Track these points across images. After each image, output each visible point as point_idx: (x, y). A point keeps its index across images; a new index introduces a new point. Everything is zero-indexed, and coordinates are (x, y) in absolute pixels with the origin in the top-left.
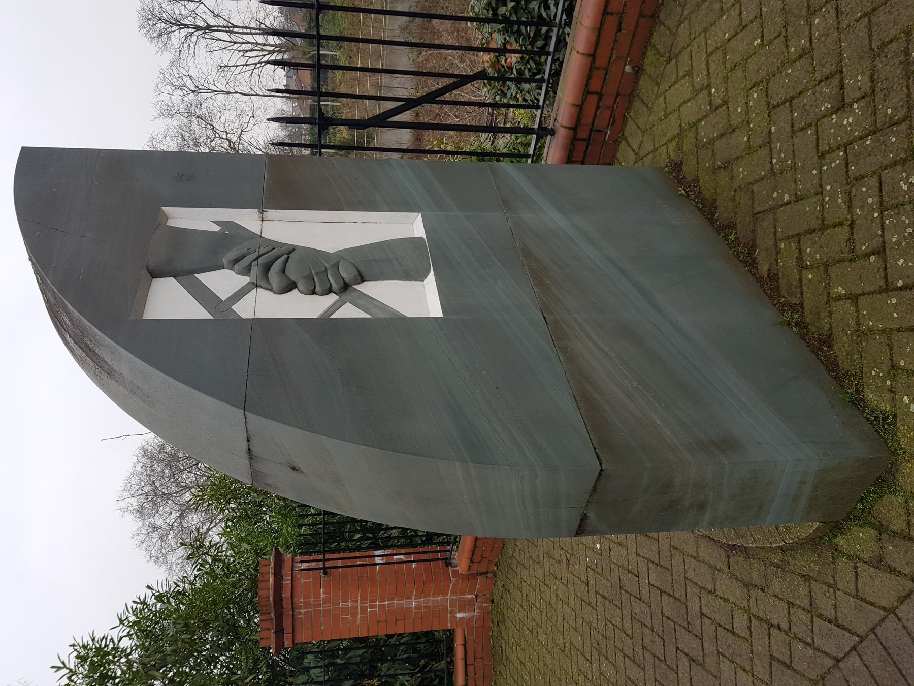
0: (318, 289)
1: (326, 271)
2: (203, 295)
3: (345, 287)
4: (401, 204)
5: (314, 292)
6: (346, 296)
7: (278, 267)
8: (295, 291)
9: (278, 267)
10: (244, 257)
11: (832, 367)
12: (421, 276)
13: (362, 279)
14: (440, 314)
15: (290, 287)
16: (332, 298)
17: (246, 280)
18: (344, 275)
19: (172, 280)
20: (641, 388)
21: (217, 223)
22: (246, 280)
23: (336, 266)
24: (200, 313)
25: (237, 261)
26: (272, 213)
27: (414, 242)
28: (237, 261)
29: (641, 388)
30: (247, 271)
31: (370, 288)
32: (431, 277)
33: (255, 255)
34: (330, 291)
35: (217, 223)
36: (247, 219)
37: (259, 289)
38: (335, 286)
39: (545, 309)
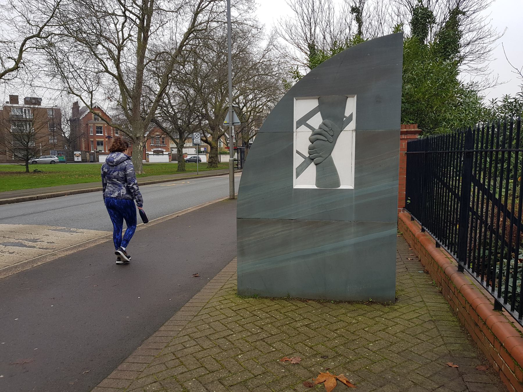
4: (358, 182)
11: (266, 298)
13: (316, 165)
16: (307, 155)
17: (317, 127)
21: (352, 114)
22: (317, 127)
26: (354, 134)
30: (320, 128)
32: (315, 187)
35: (352, 114)
36: (352, 125)
38: (311, 156)
39: (296, 221)
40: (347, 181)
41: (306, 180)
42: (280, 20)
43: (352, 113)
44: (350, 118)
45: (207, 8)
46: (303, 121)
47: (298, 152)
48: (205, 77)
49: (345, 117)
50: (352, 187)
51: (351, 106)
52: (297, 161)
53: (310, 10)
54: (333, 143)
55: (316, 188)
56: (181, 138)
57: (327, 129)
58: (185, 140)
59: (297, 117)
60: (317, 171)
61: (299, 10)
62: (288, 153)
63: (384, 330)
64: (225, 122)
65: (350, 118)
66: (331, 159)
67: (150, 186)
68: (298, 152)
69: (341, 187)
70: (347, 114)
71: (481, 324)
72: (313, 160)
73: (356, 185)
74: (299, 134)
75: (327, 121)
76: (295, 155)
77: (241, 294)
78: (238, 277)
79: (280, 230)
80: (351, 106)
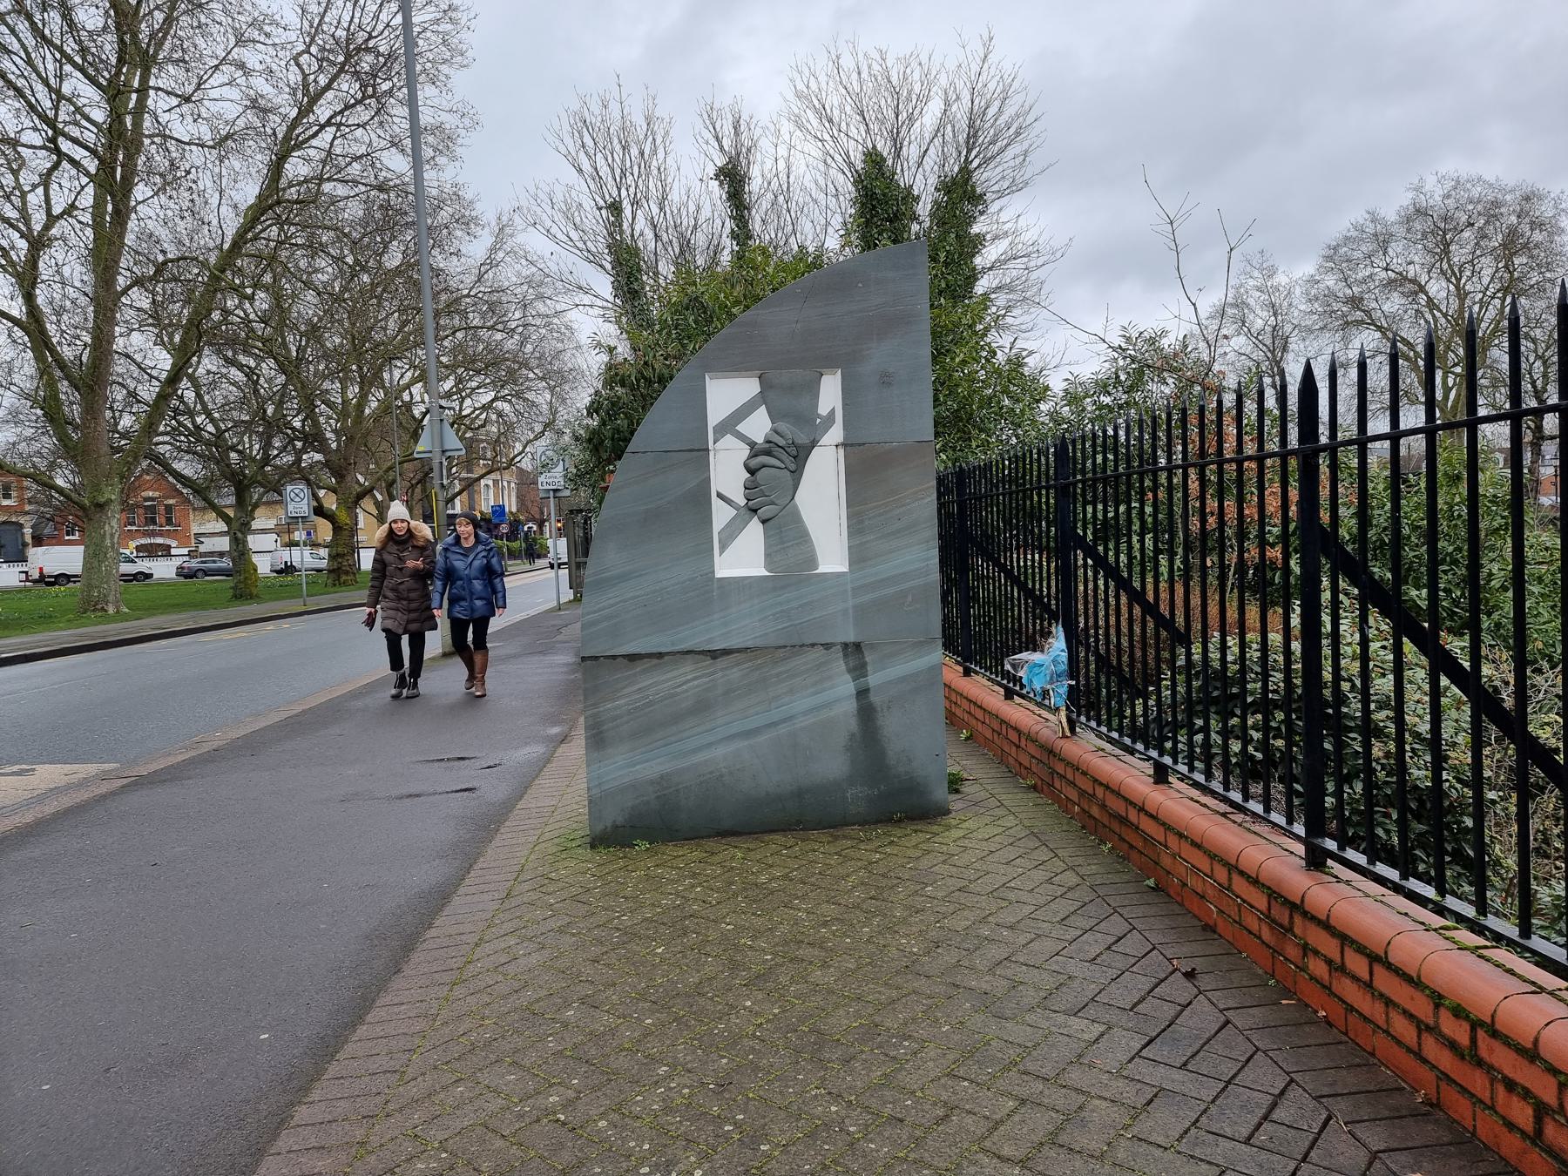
4: (858, 556)
6: (743, 511)
12: (769, 564)
13: (763, 522)
14: (718, 575)
15: (752, 472)
16: (742, 502)
17: (760, 440)
22: (760, 440)
26: (841, 451)
27: (812, 561)
36: (835, 434)
40: (832, 556)
41: (742, 557)
42: (532, 190)
44: (830, 419)
45: (314, 142)
46: (729, 426)
47: (719, 495)
48: (313, 332)
49: (819, 416)
50: (844, 568)
51: (830, 393)
52: (721, 515)
53: (618, 172)
54: (797, 474)
56: (241, 501)
57: (782, 442)
58: (256, 506)
59: (716, 413)
61: (586, 166)
62: (700, 498)
63: (944, 862)
64: (419, 448)
65: (830, 419)
66: (796, 507)
67: (163, 642)
68: (719, 495)
69: (822, 569)
70: (823, 410)
71: (1133, 816)
72: (755, 511)
73: (852, 563)
74: (720, 455)
75: (783, 426)
76: (716, 503)
77: (601, 840)
78: (590, 802)
80: (830, 393)
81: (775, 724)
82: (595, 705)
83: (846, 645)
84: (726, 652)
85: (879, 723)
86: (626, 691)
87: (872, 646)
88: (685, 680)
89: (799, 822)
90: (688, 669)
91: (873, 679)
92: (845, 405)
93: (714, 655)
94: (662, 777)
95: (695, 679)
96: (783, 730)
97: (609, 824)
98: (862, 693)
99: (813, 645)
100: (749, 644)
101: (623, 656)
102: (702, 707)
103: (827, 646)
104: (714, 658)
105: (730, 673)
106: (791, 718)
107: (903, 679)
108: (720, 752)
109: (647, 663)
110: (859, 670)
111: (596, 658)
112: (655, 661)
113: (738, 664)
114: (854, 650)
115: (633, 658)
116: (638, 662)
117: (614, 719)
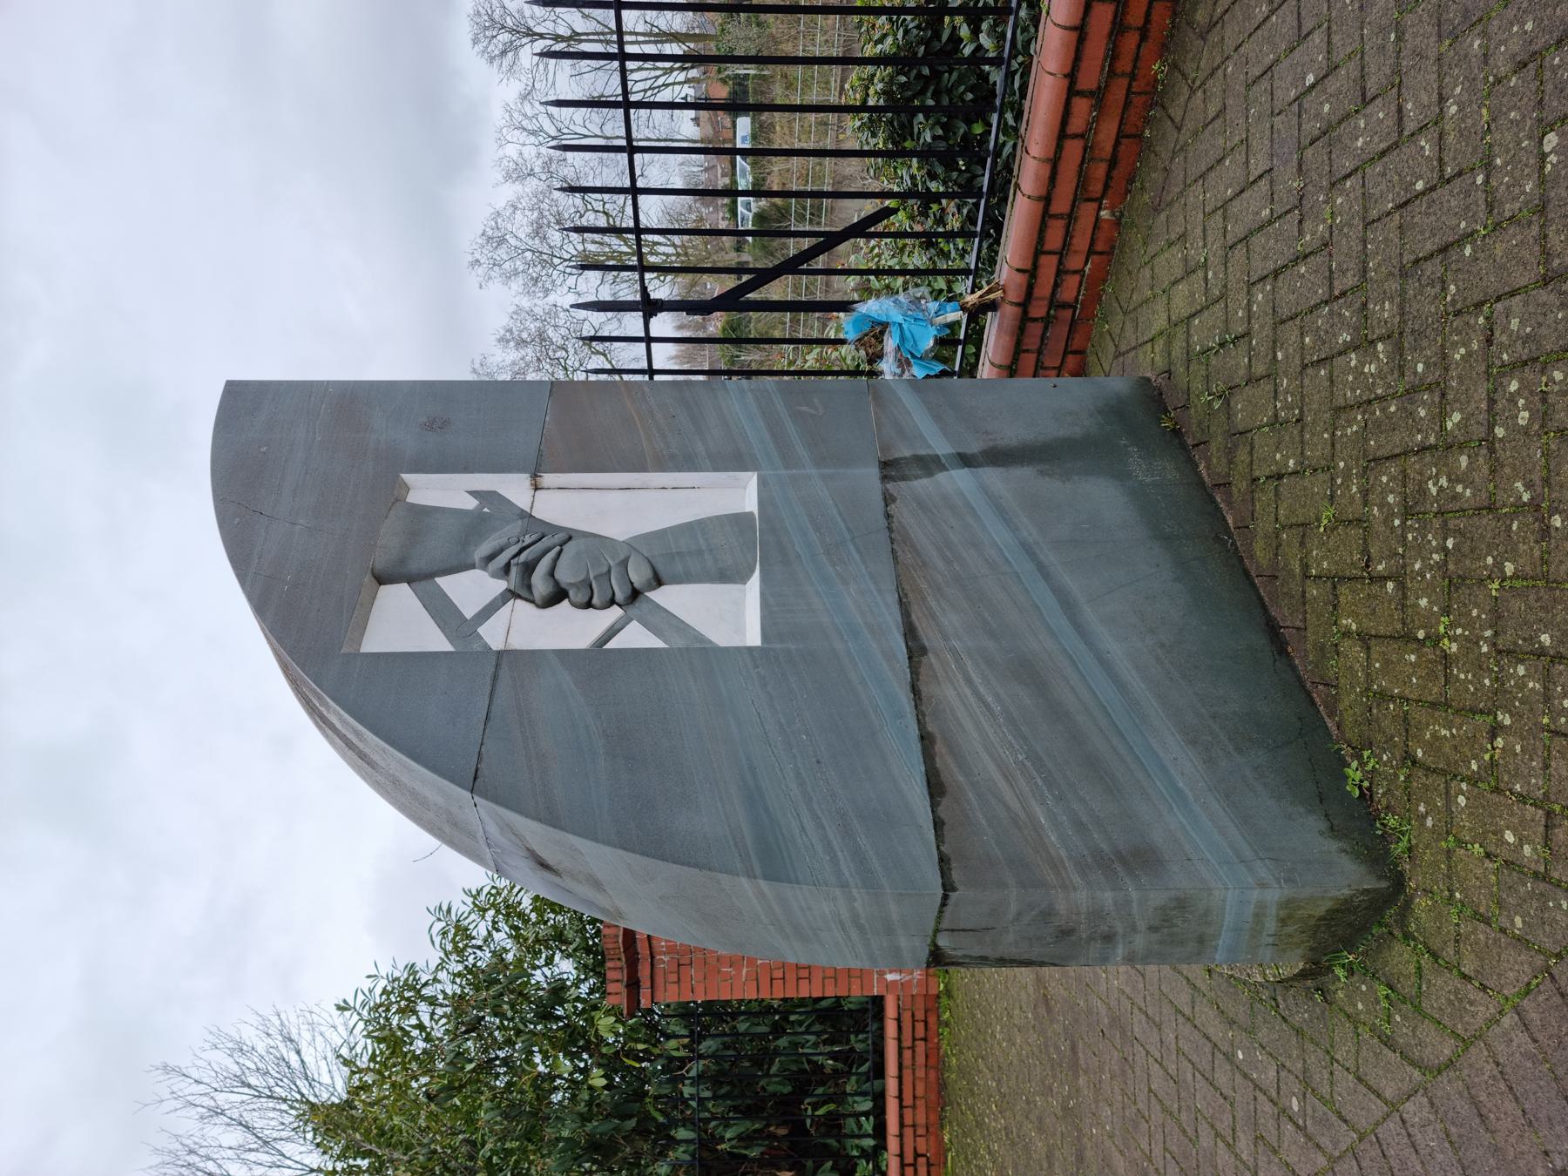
0: (595, 601)
1: (609, 571)
2: (443, 611)
3: (635, 595)
4: (734, 460)
5: (589, 605)
6: (634, 610)
7: (541, 567)
8: (566, 602)
9: (541, 567)
10: (501, 550)
12: (741, 577)
13: (658, 581)
15: (558, 596)
16: (615, 612)
17: (501, 585)
18: (634, 577)
19: (404, 588)
20: (1028, 764)
21: (473, 493)
22: (501, 585)
23: (624, 564)
24: (436, 641)
25: (491, 557)
26: (548, 479)
28: (491, 557)
29: (1028, 764)
31: (667, 597)
33: (514, 549)
34: (612, 602)
35: (473, 493)
36: (514, 488)
37: (519, 602)
38: (619, 597)
43: (471, 493)
49: (481, 507)
50: (751, 480)
52: (636, 637)
55: (755, 580)
60: (686, 578)
70: (471, 504)
73: (746, 470)
79: (968, 692)
81: (1042, 569)
82: (1055, 866)
83: (885, 478)
84: (910, 632)
85: (1014, 443)
86: (1015, 804)
87: (885, 448)
88: (971, 704)
89: (1217, 539)
90: (950, 693)
91: (941, 447)
92: (466, 469)
93: (916, 651)
94: (1193, 742)
95: (969, 681)
96: (1050, 557)
97: (1333, 845)
98: (966, 460)
99: (888, 516)
100: (892, 599)
101: (934, 806)
102: (1026, 671)
103: (888, 499)
104: (924, 651)
105: (947, 625)
106: (1028, 549)
107: (938, 418)
108: (1112, 646)
109: (944, 761)
110: (929, 465)
111: (943, 860)
112: (940, 747)
113: (933, 616)
114: (890, 469)
115: (936, 788)
116: (945, 776)
117: (1080, 826)
